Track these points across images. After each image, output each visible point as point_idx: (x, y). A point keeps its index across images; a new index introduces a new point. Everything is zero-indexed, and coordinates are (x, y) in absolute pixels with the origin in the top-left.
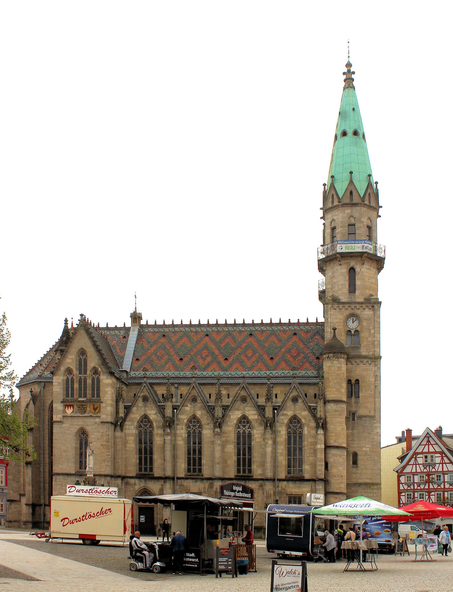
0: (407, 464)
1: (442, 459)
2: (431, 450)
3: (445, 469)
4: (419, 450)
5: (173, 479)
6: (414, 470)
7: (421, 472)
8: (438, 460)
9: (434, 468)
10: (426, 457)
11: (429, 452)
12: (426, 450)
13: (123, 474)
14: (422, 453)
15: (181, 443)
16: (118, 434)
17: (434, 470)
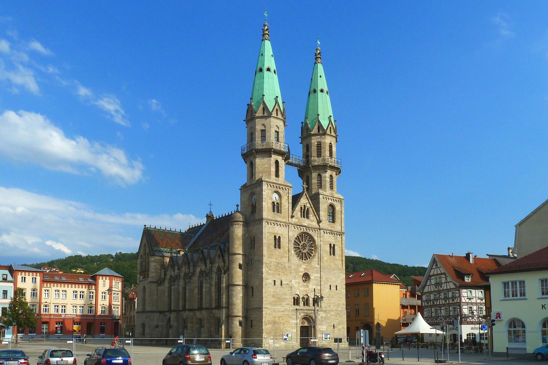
0: (425, 285)
1: (446, 279)
2: (439, 272)
3: (448, 288)
4: (432, 274)
5: (176, 311)
6: (430, 290)
7: (434, 291)
8: (443, 280)
9: (441, 287)
10: (436, 278)
11: (438, 274)
12: (435, 273)
13: (162, 310)
14: (434, 275)
15: (181, 289)
16: (159, 287)
17: (441, 289)
